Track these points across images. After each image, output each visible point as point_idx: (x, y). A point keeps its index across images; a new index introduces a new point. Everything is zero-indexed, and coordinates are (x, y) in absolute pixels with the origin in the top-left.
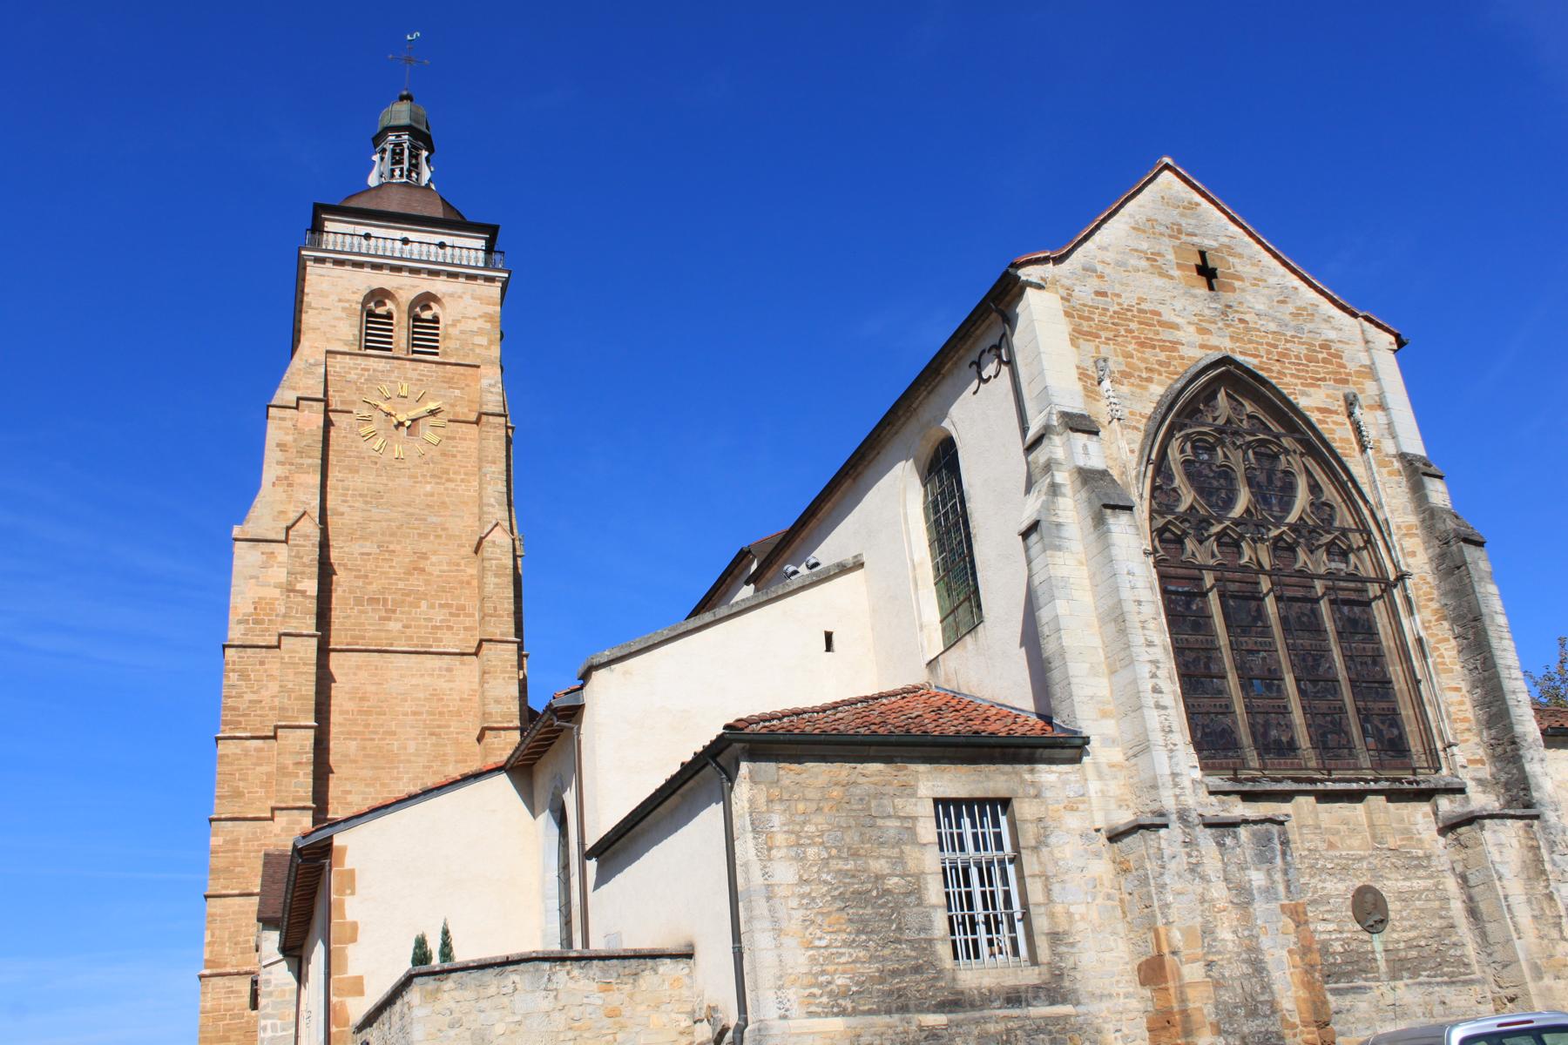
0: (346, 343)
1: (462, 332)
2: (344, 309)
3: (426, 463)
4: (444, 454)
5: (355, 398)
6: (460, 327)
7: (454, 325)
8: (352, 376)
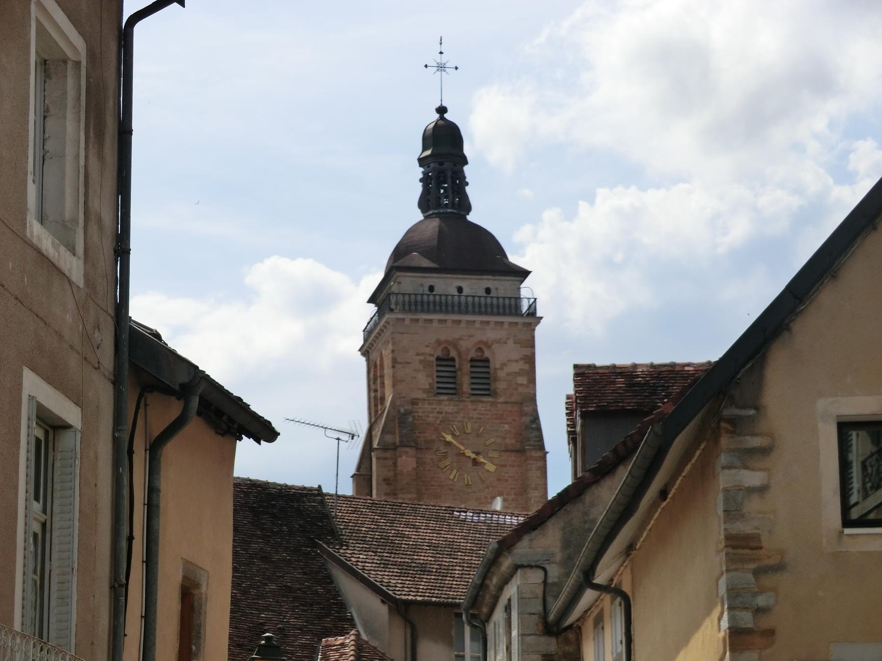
0: (425, 391)
1: (508, 374)
2: (421, 361)
3: (487, 487)
4: (499, 480)
5: (434, 437)
6: (507, 369)
7: (501, 369)
8: (431, 419)
